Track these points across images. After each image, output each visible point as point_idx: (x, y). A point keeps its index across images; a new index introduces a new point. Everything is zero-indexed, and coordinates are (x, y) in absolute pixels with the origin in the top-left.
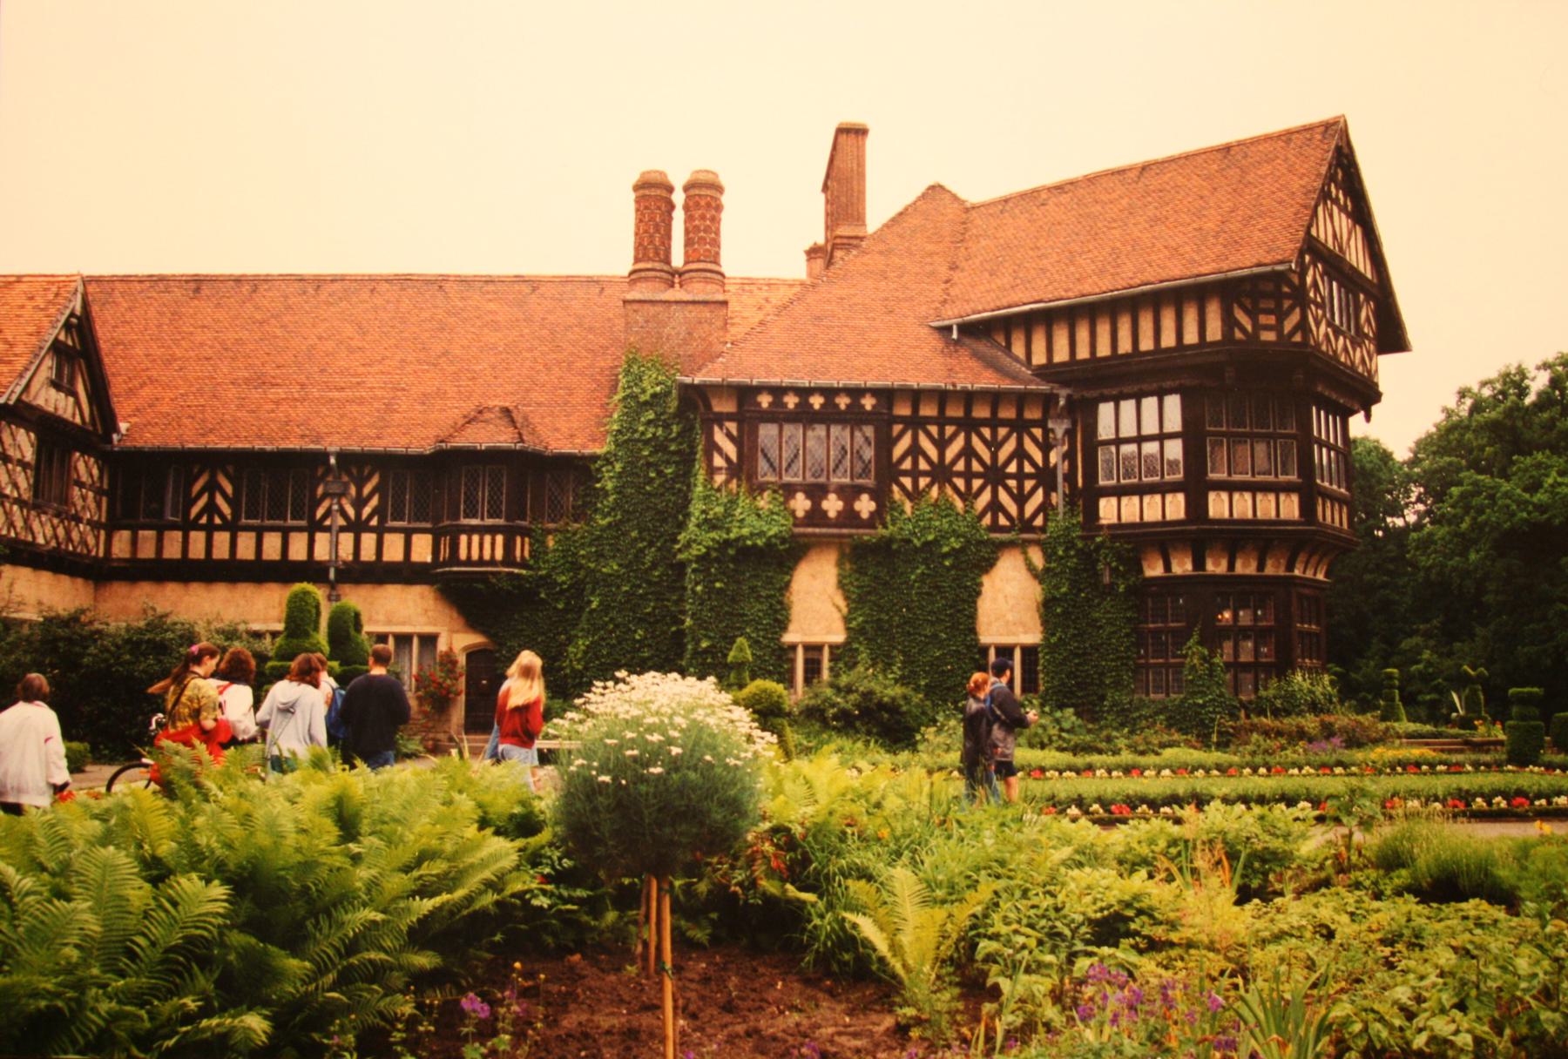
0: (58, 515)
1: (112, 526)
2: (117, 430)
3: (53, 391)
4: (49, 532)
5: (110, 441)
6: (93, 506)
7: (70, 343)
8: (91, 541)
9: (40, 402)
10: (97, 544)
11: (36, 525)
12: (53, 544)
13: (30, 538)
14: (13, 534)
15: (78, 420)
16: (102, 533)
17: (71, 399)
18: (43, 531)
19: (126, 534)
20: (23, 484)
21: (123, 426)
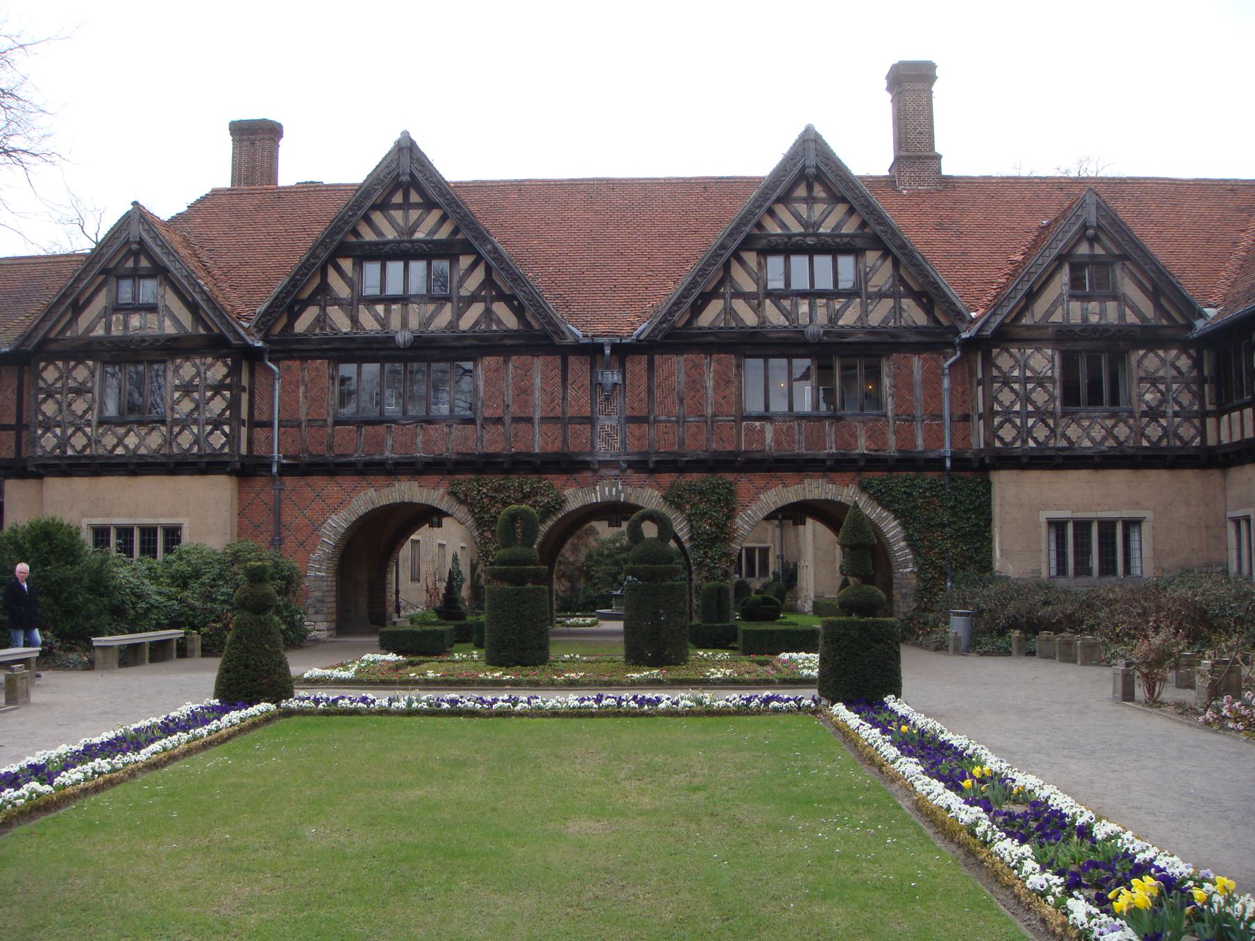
0: (1113, 415)
1: (1218, 415)
2: (1202, 315)
3: (1075, 306)
4: (1097, 433)
5: (1191, 327)
6: (1185, 398)
7: (1098, 250)
8: (1187, 431)
9: (1057, 318)
10: (1202, 432)
11: (1073, 432)
12: (1110, 443)
13: (1064, 443)
14: (1031, 444)
15: (1131, 318)
16: (1210, 423)
17: (1111, 306)
18: (1086, 432)
19: (1226, 417)
20: (1040, 397)
21: (1211, 312)
